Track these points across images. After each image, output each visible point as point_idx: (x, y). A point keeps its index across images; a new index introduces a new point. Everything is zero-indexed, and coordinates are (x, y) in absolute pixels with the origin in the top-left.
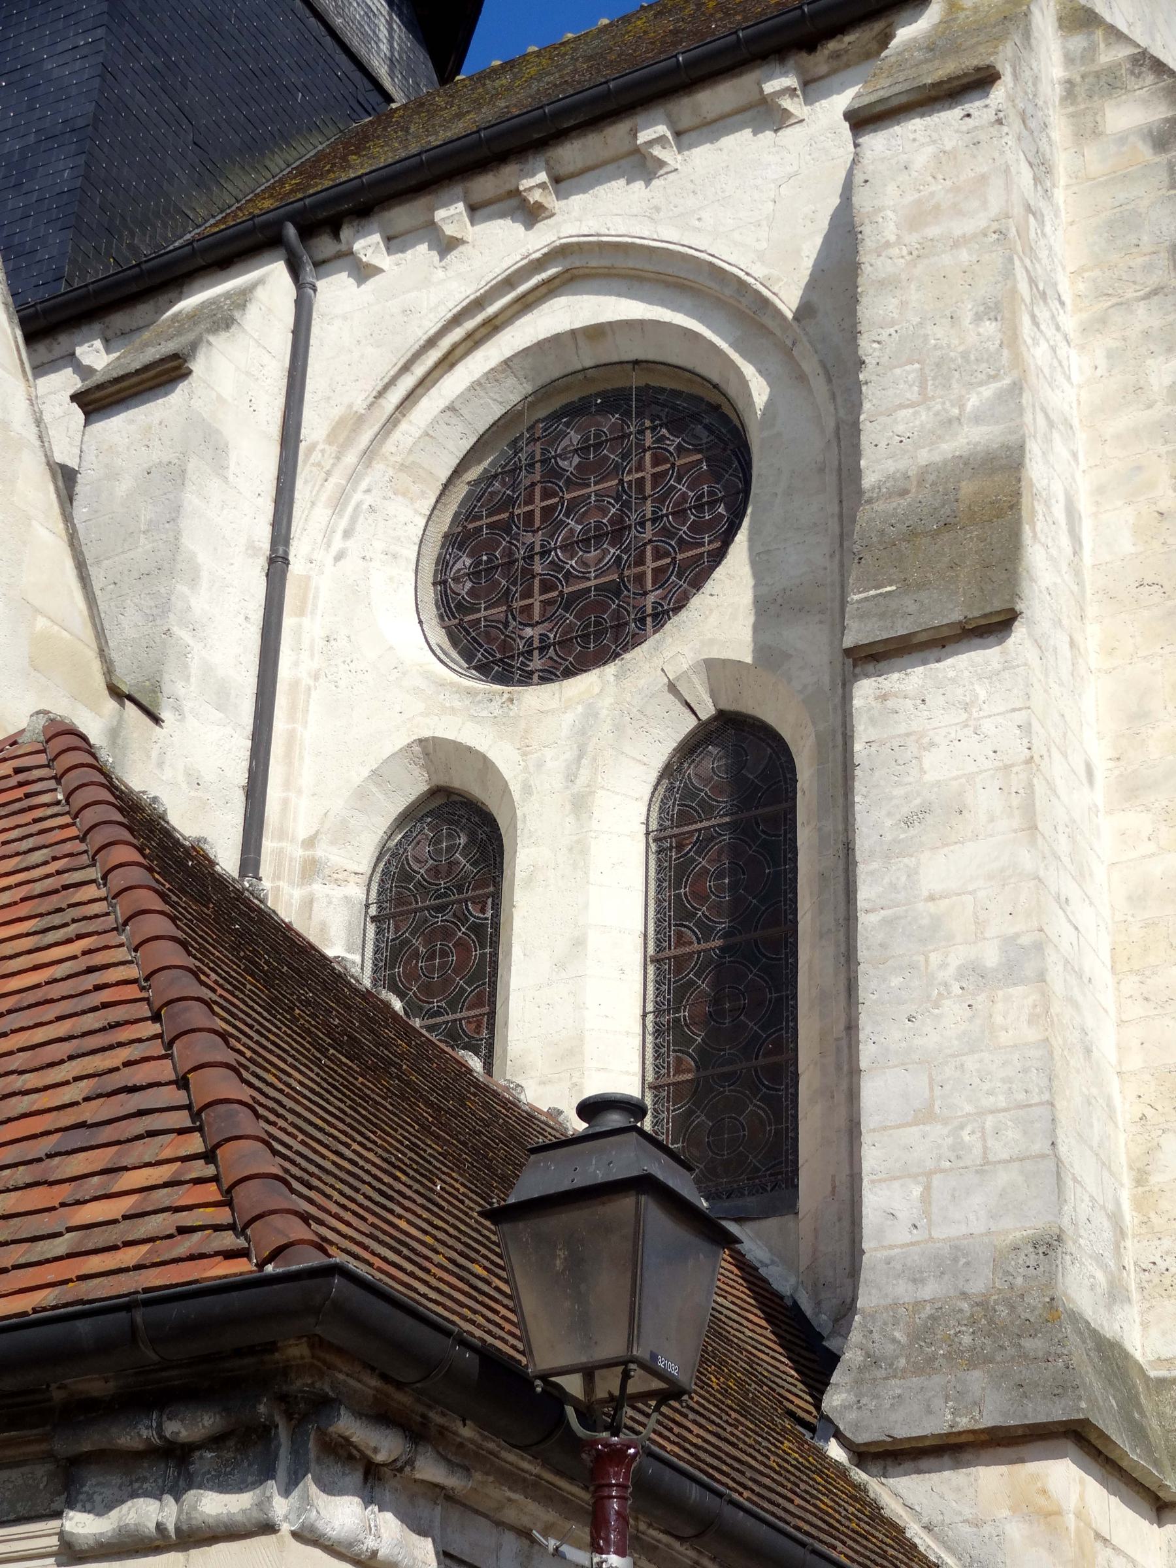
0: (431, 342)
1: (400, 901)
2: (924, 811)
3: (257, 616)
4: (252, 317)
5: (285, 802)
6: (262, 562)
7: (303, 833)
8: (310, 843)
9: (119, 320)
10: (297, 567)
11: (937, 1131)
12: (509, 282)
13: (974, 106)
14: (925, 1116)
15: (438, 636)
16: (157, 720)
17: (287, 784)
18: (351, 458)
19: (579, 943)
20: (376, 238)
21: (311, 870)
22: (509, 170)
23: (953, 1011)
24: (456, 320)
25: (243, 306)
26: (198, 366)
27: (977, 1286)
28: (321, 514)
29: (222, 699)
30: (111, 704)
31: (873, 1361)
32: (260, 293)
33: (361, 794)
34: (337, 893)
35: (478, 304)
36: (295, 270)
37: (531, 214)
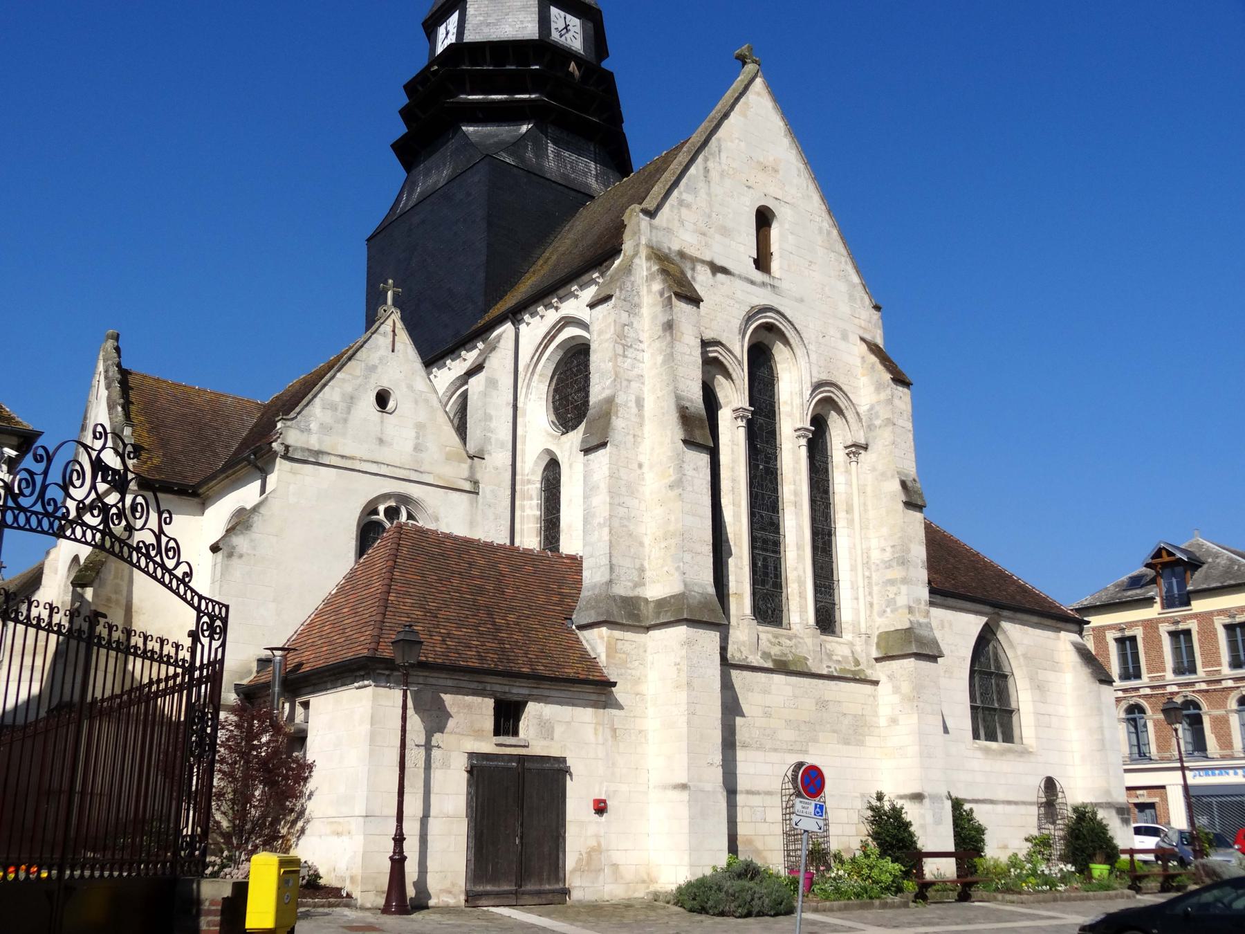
0: (541, 344)
1: (548, 486)
2: (593, 487)
3: (511, 420)
4: (502, 343)
5: (522, 467)
6: (511, 405)
7: (526, 473)
8: (528, 475)
9: (484, 336)
10: (520, 405)
11: (594, 559)
12: (554, 327)
13: (609, 303)
14: (592, 556)
15: (553, 418)
16: (483, 459)
17: (523, 462)
18: (529, 375)
19: (571, 500)
20: (527, 315)
21: (529, 482)
22: (550, 297)
23: (596, 533)
24: (545, 337)
25: (499, 341)
26: (486, 365)
27: (596, 592)
28: (524, 390)
29: (502, 446)
30: (469, 460)
31: (580, 608)
32: (504, 335)
33: (536, 462)
34: (534, 486)
35: (548, 333)
36: (513, 324)
37: (557, 309)
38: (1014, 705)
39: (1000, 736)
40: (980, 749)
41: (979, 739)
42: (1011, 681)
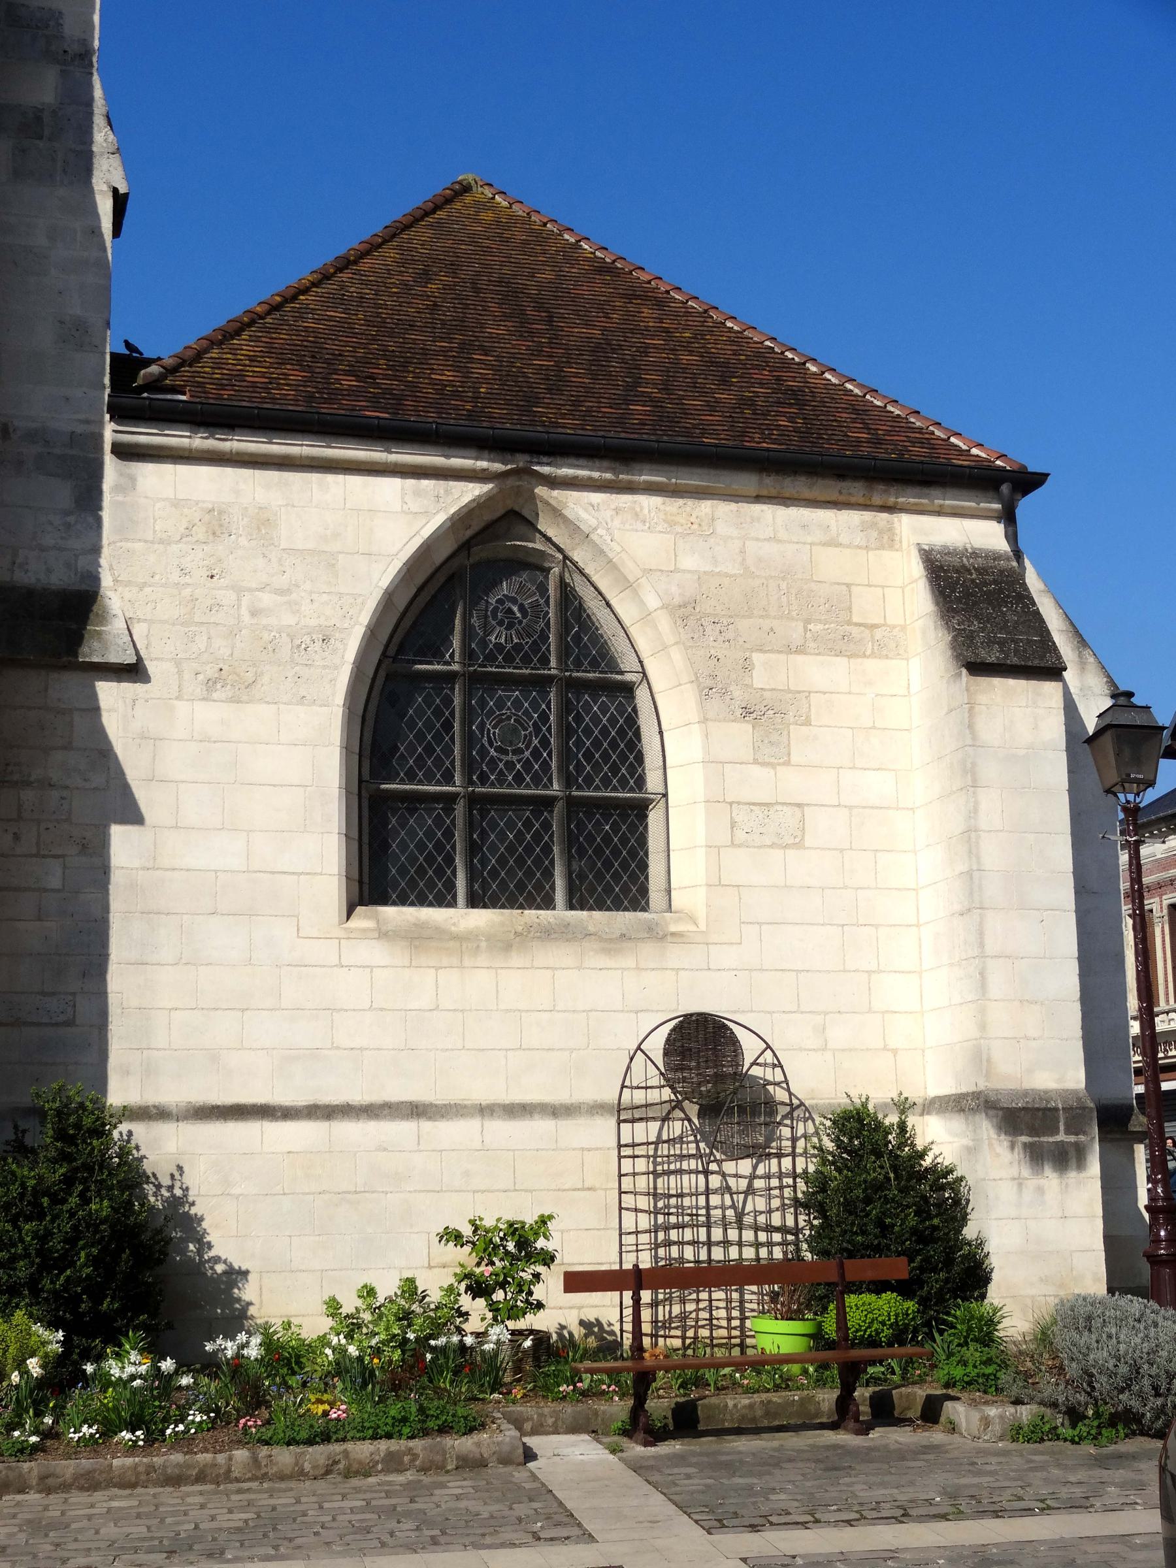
38: (653, 782)
39: (560, 896)
40: (384, 934)
41: (452, 904)
42: (641, 695)
